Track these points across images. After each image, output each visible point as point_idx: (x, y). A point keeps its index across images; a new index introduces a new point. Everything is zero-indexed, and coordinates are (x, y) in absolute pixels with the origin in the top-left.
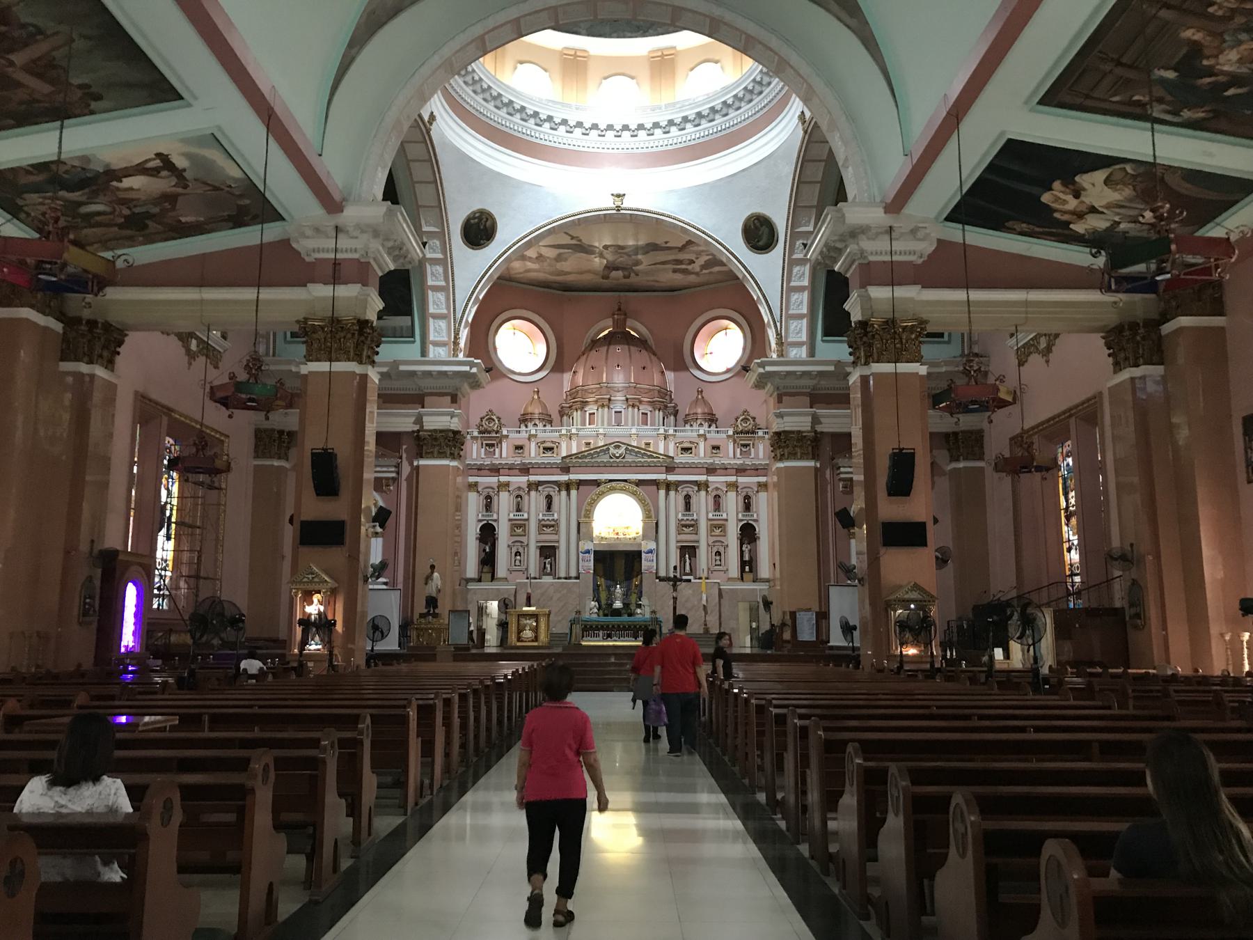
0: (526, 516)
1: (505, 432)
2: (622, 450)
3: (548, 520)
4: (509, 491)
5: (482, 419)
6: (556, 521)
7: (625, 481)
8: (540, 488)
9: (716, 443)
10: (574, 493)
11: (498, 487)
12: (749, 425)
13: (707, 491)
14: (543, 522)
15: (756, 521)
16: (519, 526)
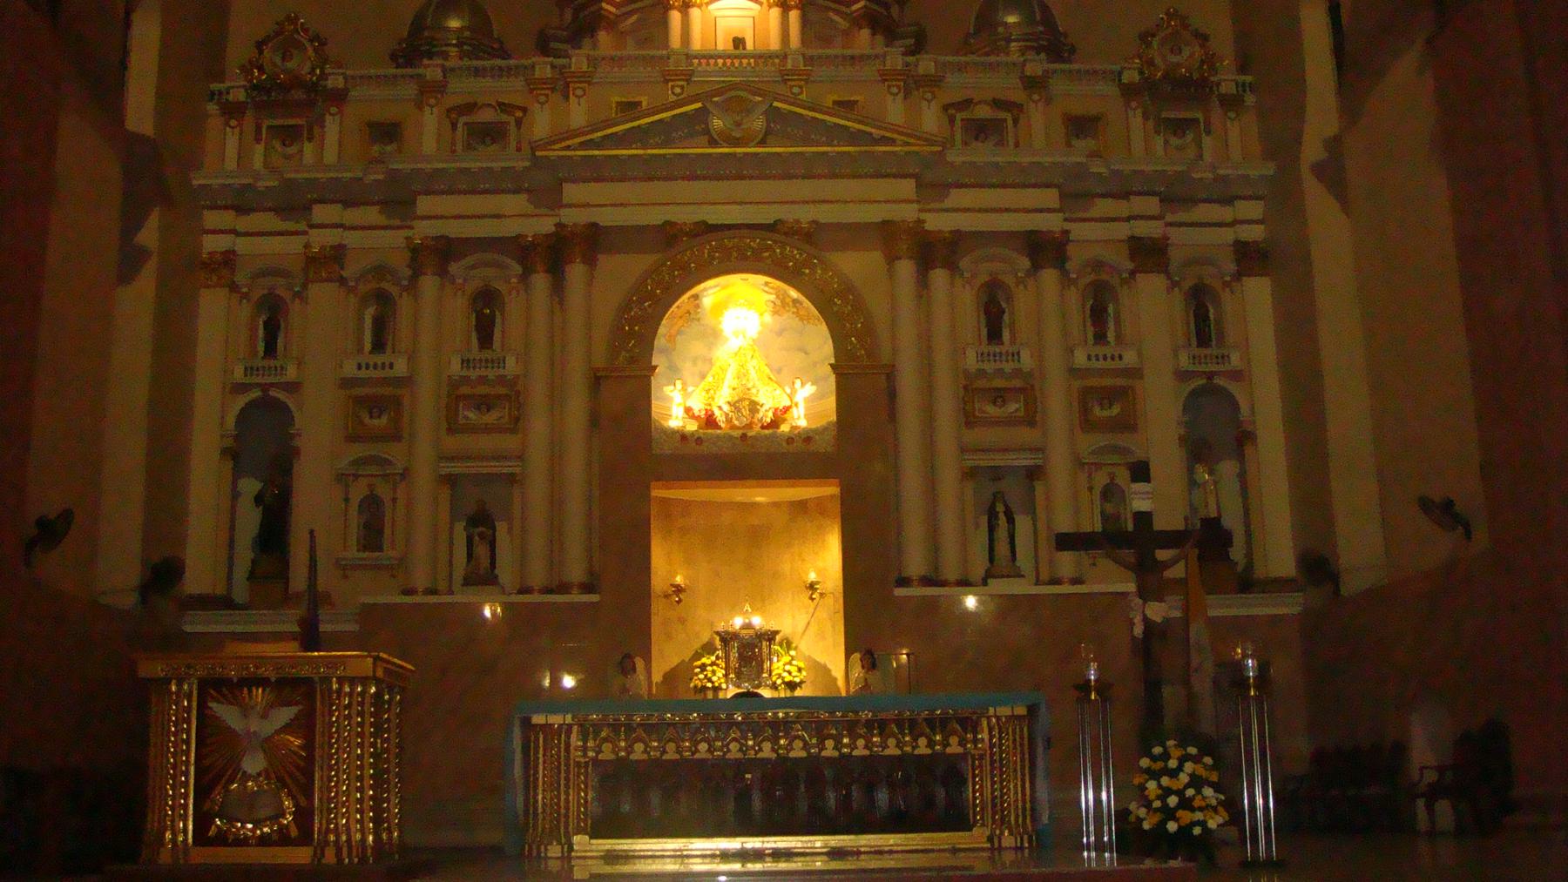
0: (401, 368)
1: (335, 82)
2: (758, 123)
3: (482, 380)
4: (342, 281)
5: (260, 45)
6: (512, 383)
7: (771, 228)
8: (454, 268)
9: (1078, 109)
10: (576, 272)
11: (306, 269)
12: (1188, 57)
13: (1065, 273)
14: (465, 390)
15: (1237, 375)
16: (375, 405)
